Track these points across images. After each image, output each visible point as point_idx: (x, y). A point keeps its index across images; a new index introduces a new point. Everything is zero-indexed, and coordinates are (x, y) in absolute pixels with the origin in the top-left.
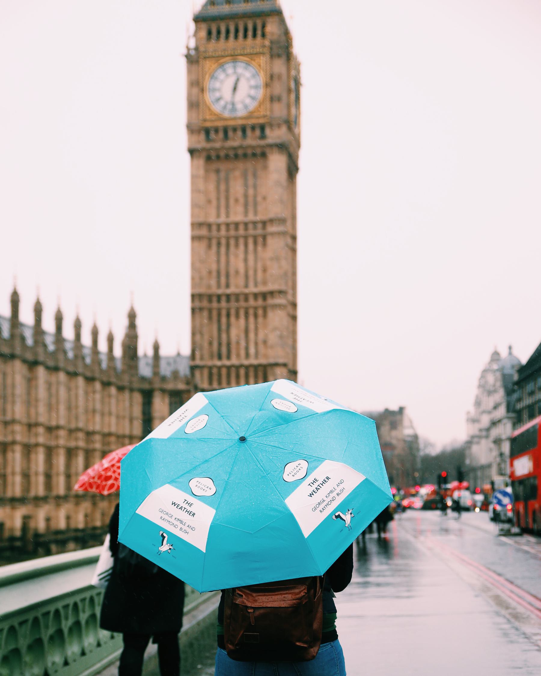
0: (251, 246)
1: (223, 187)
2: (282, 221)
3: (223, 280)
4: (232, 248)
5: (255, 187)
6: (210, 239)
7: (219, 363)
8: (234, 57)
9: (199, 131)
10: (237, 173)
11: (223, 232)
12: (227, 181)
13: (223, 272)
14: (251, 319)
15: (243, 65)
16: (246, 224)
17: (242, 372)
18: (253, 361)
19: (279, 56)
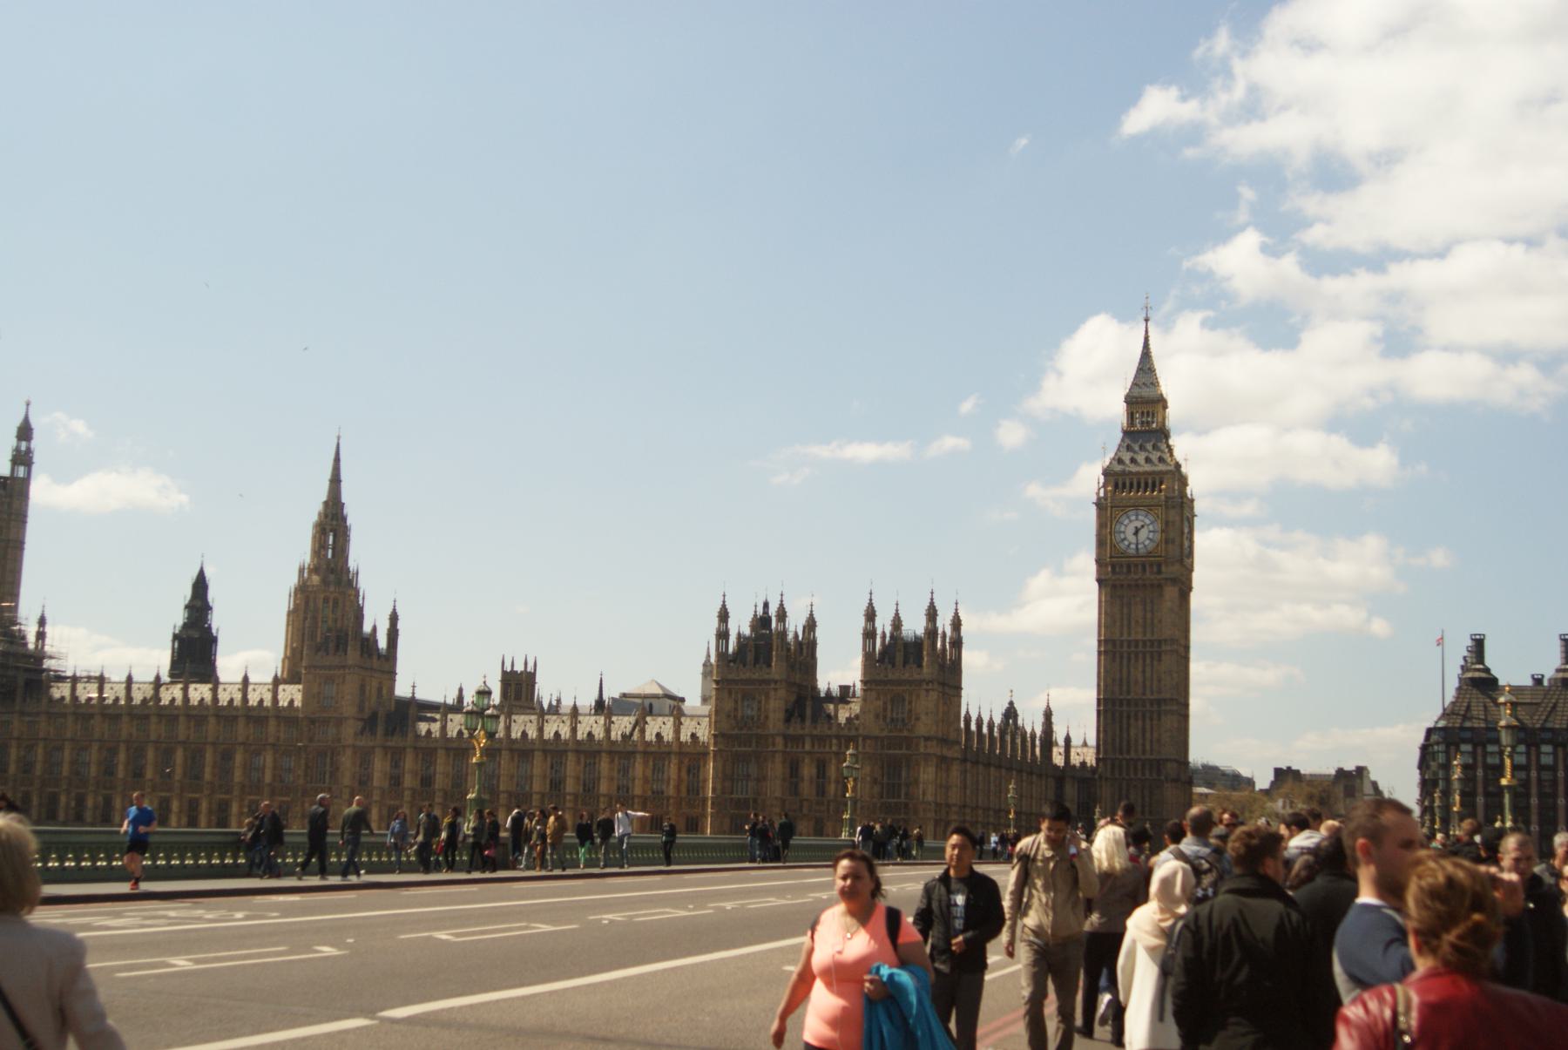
0: (1148, 661)
1: (1125, 610)
2: (1173, 641)
3: (1125, 688)
4: (1133, 661)
5: (1152, 611)
6: (1114, 654)
7: (1121, 757)
8: (1136, 507)
10: (1138, 599)
11: (1125, 649)
13: (1125, 682)
14: (1148, 722)
15: (1143, 513)
16: (1144, 642)
17: (1139, 764)
18: (1148, 756)
19: (1174, 507)
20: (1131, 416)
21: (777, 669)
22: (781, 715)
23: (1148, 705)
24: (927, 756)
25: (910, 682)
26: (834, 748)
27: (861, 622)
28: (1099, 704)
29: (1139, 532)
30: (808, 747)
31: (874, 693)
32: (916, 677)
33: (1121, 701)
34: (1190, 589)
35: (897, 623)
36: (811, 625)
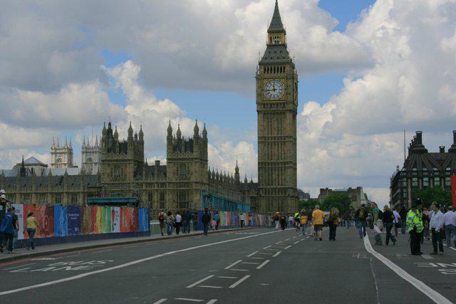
3: (270, 157)
8: (274, 79)
9: (261, 104)
12: (271, 122)
14: (280, 171)
20: (271, 39)
21: (130, 156)
22: (132, 174)
23: (280, 165)
24: (197, 190)
25: (188, 159)
26: (156, 188)
27: (166, 134)
28: (259, 165)
29: (276, 90)
30: (144, 188)
31: (173, 164)
32: (190, 157)
33: (269, 163)
34: (296, 114)
35: (179, 133)
36: (141, 134)
